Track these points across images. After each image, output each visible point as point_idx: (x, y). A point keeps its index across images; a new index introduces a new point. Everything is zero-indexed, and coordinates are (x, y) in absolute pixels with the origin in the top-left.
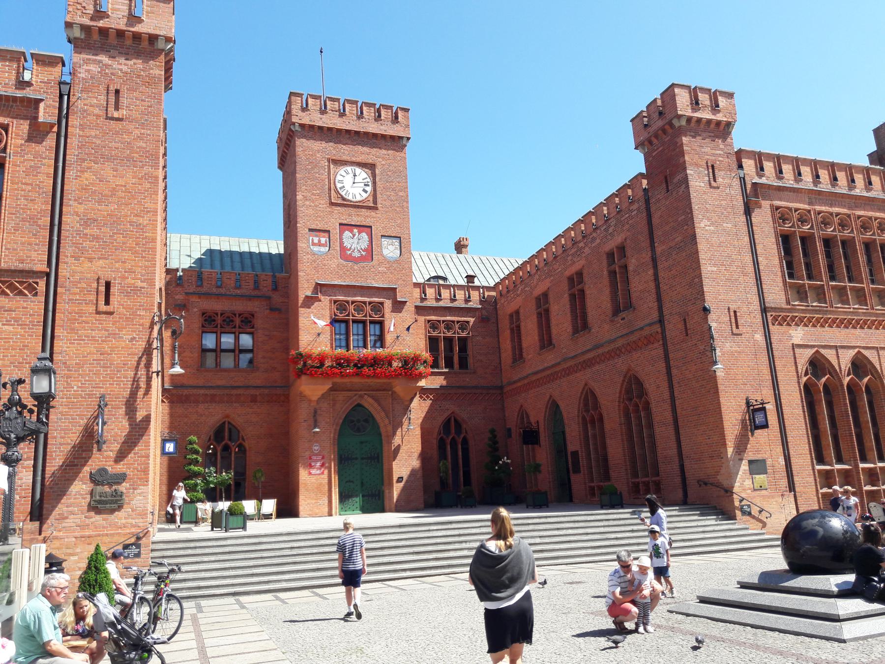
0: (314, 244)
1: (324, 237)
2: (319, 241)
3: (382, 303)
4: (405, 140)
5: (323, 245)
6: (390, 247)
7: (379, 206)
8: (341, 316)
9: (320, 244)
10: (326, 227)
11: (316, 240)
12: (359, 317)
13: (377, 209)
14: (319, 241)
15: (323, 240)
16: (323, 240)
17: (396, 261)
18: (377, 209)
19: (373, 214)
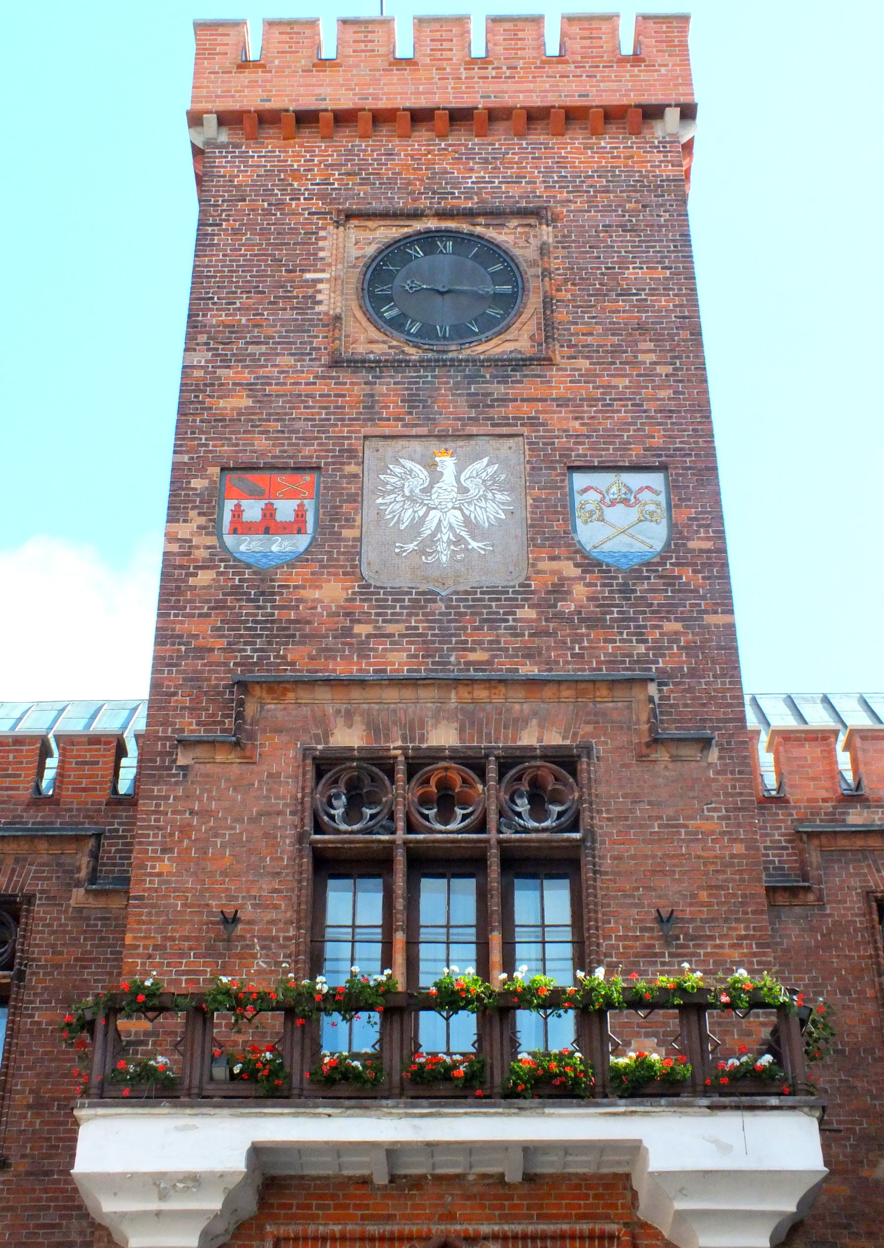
0: (240, 527)
1: (291, 495)
2: (269, 513)
3: (567, 761)
4: (672, 115)
5: (285, 529)
6: (619, 515)
7: (559, 353)
8: (346, 832)
9: (269, 525)
10: (309, 452)
11: (253, 510)
12: (451, 831)
13: (548, 361)
14: (269, 513)
15: (285, 509)
16: (285, 509)
17: (650, 566)
18: (548, 361)
19: (529, 388)
